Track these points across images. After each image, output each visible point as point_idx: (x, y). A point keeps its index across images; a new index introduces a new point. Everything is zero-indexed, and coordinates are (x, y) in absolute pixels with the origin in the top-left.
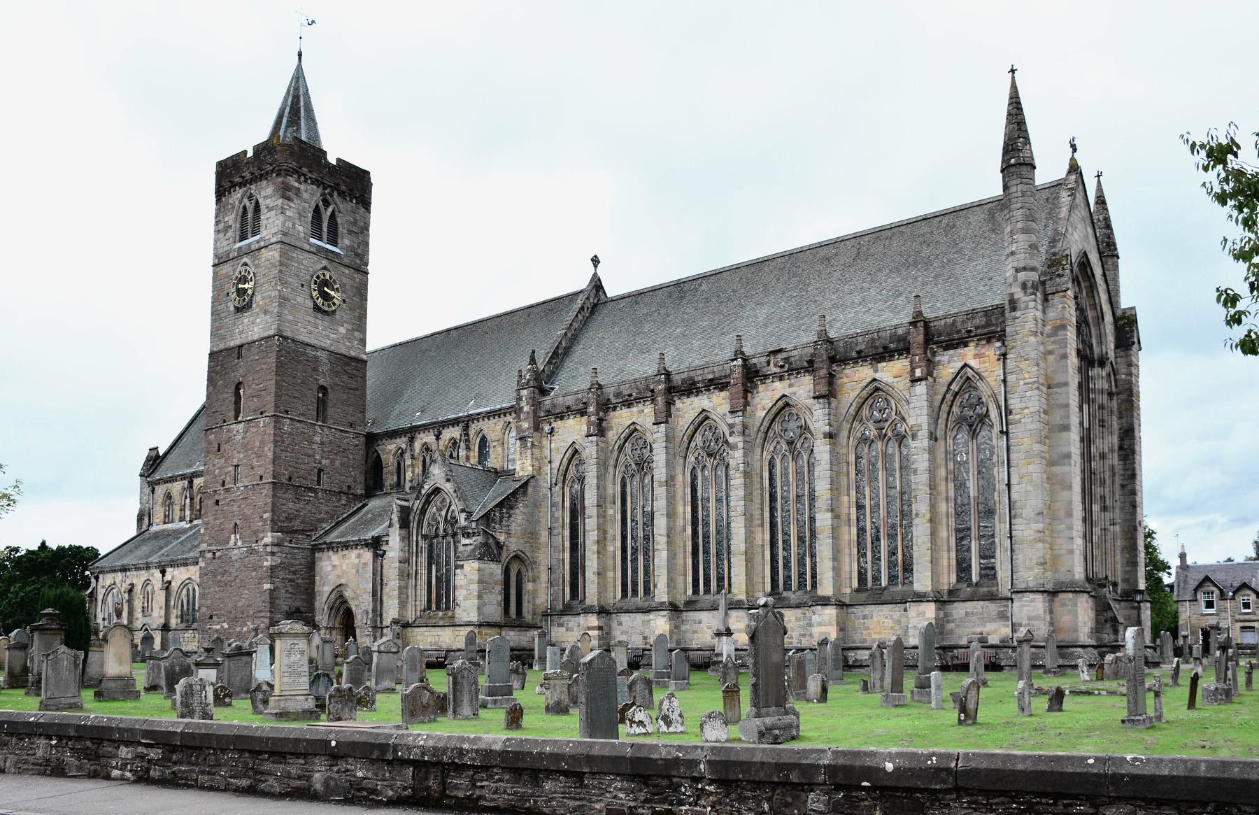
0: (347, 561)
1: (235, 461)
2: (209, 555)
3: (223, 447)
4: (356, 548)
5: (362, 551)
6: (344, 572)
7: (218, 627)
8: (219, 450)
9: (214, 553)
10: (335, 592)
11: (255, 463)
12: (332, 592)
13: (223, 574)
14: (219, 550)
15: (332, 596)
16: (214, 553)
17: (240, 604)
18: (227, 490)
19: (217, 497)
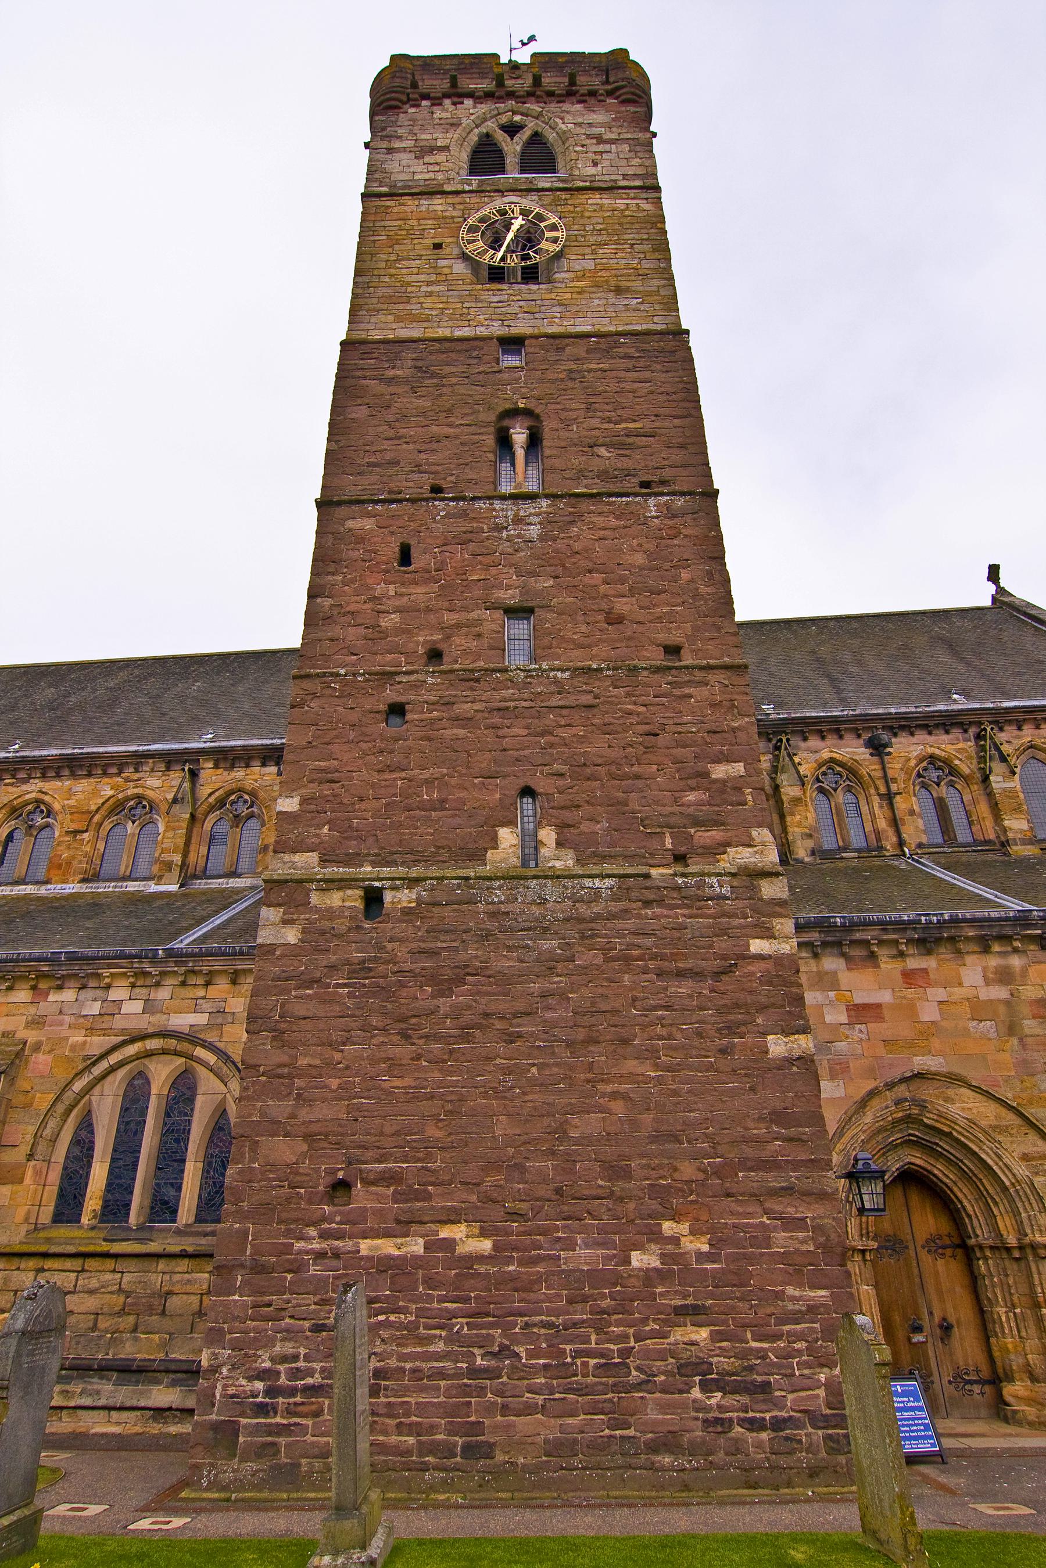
0: (938, 993)
1: (510, 596)
2: (353, 899)
3: (419, 560)
4: (986, 950)
5: (1016, 962)
6: (929, 1031)
7: (416, 1246)
8: (405, 557)
9: (373, 899)
10: (876, 1103)
11: (623, 606)
12: (863, 1104)
13: (444, 986)
14: (412, 882)
15: (868, 1118)
16: (373, 899)
17: (588, 1125)
18: (471, 678)
19: (391, 695)
